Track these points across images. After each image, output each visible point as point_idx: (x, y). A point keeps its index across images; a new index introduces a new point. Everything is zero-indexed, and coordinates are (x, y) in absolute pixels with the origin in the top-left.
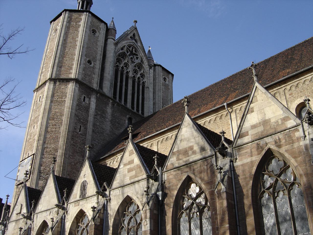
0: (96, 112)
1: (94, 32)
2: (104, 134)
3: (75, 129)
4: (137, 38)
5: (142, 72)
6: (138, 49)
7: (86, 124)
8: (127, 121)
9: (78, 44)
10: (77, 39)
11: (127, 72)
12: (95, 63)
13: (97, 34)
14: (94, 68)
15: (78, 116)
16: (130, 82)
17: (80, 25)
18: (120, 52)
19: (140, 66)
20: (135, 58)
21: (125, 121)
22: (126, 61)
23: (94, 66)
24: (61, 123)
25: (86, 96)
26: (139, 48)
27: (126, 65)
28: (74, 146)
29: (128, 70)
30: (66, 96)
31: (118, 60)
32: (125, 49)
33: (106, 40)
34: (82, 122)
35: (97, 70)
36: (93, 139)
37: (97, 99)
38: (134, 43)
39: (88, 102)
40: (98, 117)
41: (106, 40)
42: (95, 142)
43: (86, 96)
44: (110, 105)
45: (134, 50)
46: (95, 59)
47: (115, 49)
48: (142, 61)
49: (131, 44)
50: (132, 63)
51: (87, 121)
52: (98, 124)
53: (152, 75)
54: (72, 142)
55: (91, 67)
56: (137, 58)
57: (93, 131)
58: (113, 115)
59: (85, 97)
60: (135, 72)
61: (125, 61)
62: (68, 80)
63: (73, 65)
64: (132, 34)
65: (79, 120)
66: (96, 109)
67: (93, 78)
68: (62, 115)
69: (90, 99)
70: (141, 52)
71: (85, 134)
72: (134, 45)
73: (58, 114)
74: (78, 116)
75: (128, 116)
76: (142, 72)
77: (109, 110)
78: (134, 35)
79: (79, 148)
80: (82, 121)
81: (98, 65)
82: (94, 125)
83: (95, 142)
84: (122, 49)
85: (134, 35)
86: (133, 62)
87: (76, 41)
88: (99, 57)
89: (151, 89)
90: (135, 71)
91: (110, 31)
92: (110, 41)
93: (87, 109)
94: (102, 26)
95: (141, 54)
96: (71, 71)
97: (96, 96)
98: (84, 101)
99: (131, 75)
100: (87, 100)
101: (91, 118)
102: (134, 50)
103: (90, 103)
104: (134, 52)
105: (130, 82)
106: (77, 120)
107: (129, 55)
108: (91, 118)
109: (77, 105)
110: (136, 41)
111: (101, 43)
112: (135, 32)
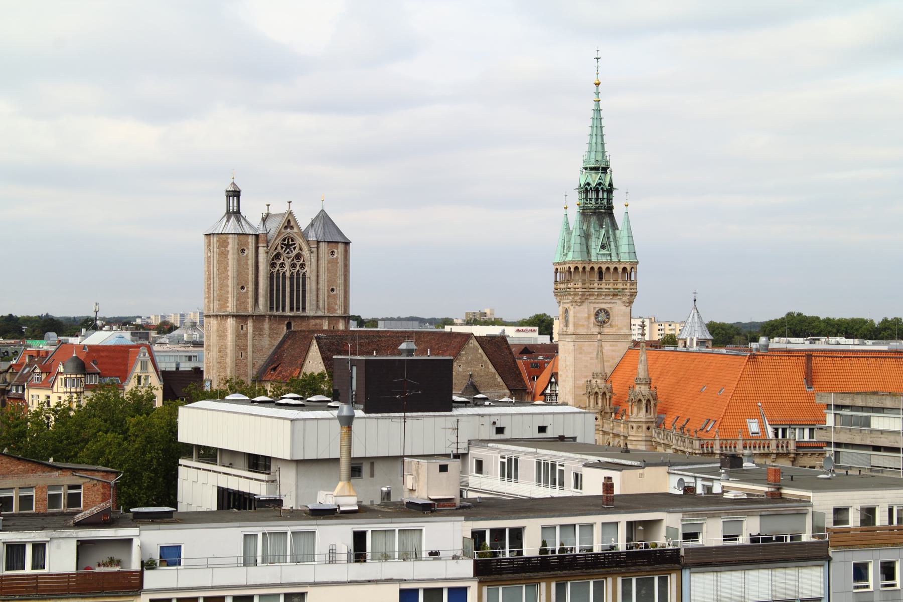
0: (254, 334)
1: (243, 251)
2: (264, 350)
3: (238, 357)
4: (292, 223)
5: (301, 262)
7: (247, 349)
8: (285, 328)
9: (230, 273)
10: (228, 268)
11: (284, 273)
12: (248, 286)
13: (246, 252)
14: (247, 292)
15: (238, 346)
16: (288, 282)
17: (228, 251)
18: (274, 254)
19: (298, 256)
20: (292, 249)
21: (283, 328)
22: (281, 261)
23: (247, 290)
24: (226, 355)
25: (243, 324)
26: (295, 235)
27: (282, 265)
28: (238, 370)
29: (284, 270)
30: (227, 331)
31: (273, 265)
32: (279, 247)
33: (257, 248)
34: (243, 349)
35: (251, 294)
36: (253, 358)
37: (254, 321)
39: (245, 329)
40: (256, 338)
41: (257, 248)
42: (256, 360)
43: (243, 324)
44: (267, 320)
45: (290, 240)
46: (247, 282)
47: (267, 257)
48: (301, 249)
49: (287, 236)
51: (247, 346)
52: (257, 344)
53: (314, 260)
54: (237, 369)
55: (245, 292)
56: (294, 248)
57: (253, 352)
58: (270, 329)
59: (242, 326)
60: (293, 266)
61: (279, 263)
62: (227, 316)
63: (228, 298)
64: (286, 224)
65: (240, 348)
66: (253, 331)
67: (248, 303)
68: (226, 348)
69: (247, 325)
70: (299, 239)
71: (247, 358)
73: (224, 347)
74: (238, 346)
75: (286, 322)
76: (301, 262)
77: (266, 325)
79: (243, 370)
80: (242, 348)
81: (251, 287)
82: (254, 346)
83: (256, 360)
84: (276, 248)
85: (289, 221)
86: (288, 258)
87: (228, 271)
88: (251, 277)
89: (314, 278)
91: (260, 237)
92: (262, 250)
93: (246, 335)
94: (250, 237)
95: (299, 241)
96: (228, 304)
97: (253, 319)
98: (242, 329)
99: (288, 274)
100: (244, 328)
101: (250, 343)
102: (290, 240)
103: (247, 329)
104: (290, 243)
105: (288, 282)
106: (238, 349)
107: (285, 251)
108: (250, 343)
109: (237, 336)
110: (292, 228)
111: (251, 262)
112: (290, 218)
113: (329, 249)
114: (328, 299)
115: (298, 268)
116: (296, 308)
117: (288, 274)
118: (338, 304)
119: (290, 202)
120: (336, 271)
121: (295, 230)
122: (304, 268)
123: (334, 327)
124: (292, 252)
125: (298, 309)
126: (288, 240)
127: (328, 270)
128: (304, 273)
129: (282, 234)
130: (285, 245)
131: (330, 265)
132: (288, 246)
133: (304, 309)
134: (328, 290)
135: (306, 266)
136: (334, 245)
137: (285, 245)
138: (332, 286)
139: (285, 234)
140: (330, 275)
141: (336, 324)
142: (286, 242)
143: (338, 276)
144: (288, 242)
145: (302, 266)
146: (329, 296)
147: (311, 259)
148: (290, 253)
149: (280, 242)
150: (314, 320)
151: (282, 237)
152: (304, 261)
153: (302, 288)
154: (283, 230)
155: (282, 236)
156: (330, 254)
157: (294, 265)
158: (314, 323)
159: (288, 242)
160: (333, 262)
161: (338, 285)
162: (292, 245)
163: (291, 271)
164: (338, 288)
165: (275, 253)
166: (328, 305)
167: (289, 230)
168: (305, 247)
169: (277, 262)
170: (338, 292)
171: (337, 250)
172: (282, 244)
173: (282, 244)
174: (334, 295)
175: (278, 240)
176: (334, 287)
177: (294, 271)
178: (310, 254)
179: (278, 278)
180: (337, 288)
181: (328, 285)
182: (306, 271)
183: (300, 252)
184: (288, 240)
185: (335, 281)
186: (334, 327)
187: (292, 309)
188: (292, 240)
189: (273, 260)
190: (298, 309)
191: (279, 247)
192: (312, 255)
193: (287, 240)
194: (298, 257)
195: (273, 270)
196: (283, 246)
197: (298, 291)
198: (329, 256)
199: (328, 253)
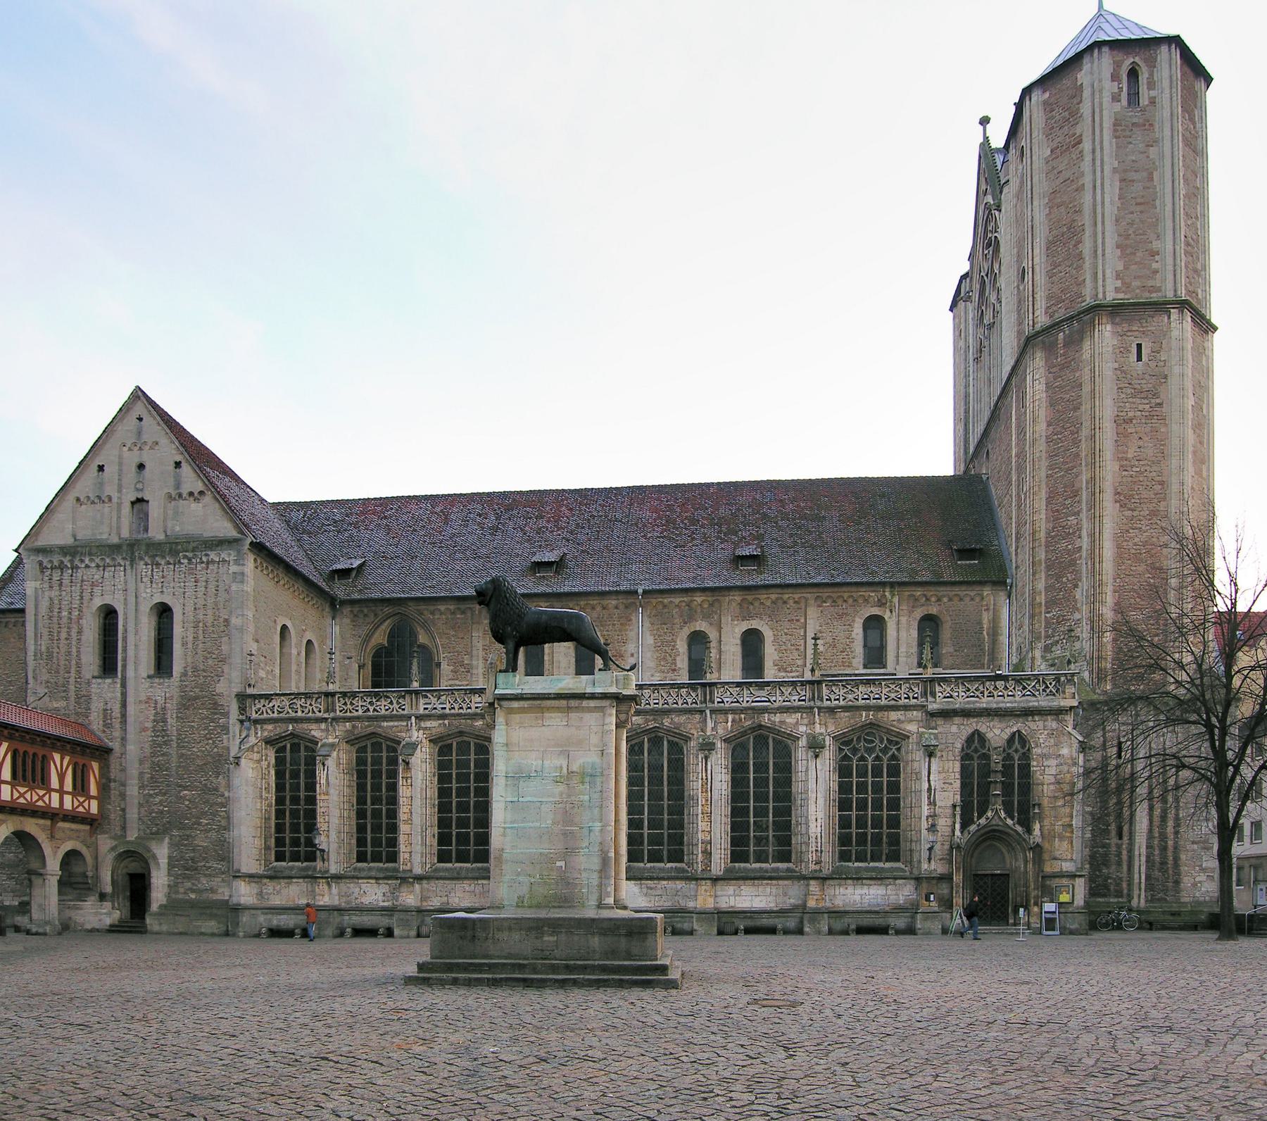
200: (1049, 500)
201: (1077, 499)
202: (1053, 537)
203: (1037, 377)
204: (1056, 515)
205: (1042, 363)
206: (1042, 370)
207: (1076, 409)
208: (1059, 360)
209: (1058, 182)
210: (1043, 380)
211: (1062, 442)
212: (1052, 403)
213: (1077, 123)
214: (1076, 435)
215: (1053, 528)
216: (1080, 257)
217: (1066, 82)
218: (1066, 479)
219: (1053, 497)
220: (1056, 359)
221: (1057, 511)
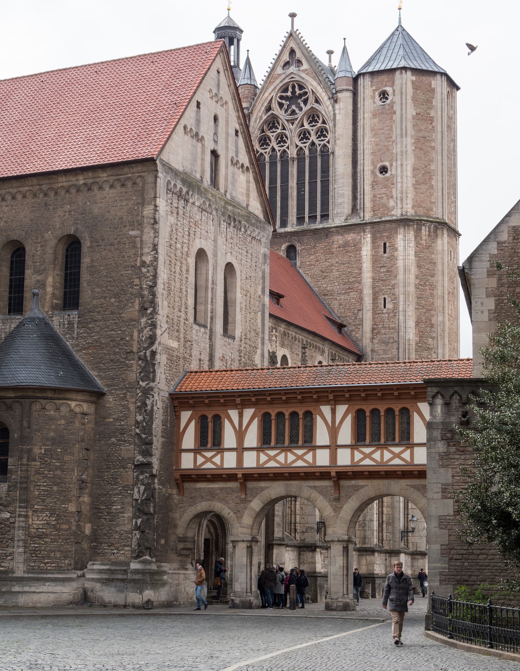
4: (299, 55)
6: (303, 78)
20: (302, 105)
26: (303, 75)
38: (292, 73)
49: (287, 80)
50: (293, 124)
56: (305, 102)
60: (304, 135)
72: (292, 78)
75: (284, 247)
78: (292, 52)
85: (292, 52)
90: (305, 134)
104: (298, 92)
112: (292, 44)
113: (374, 88)
114: (373, 188)
115: (313, 138)
116: (309, 217)
117: (292, 153)
118: (395, 196)
119: (293, 16)
120: (391, 129)
121: (305, 66)
122: (325, 136)
123: (385, 244)
124: (301, 109)
125: (312, 218)
126: (294, 87)
127: (372, 130)
128: (325, 145)
129: (277, 78)
130: (286, 98)
131: (376, 120)
132: (293, 99)
133: (325, 216)
134: (373, 172)
135: (329, 133)
136: (384, 78)
137: (286, 98)
138: (381, 161)
139: (283, 76)
140: (376, 140)
141: (389, 237)
142: (289, 94)
143: (394, 138)
144: (293, 92)
145: (322, 133)
146: (374, 184)
147: (335, 115)
148: (297, 111)
149: (274, 94)
150: (341, 235)
151: (278, 83)
152: (324, 122)
153: (322, 177)
154: (279, 70)
155: (278, 81)
156: (377, 98)
157: (305, 134)
158: (341, 242)
159: (293, 92)
160: (382, 113)
161: (395, 159)
162: (300, 96)
163: (297, 146)
164: (394, 164)
165: (264, 117)
166: (373, 201)
167: (292, 69)
168: (324, 94)
169: (270, 135)
170: (394, 172)
171: (392, 86)
172: (281, 98)
173: (281, 98)
174: (387, 179)
175: (269, 90)
176: (387, 164)
177: (302, 145)
178: (333, 107)
179: (273, 164)
180: (391, 165)
181: (373, 163)
182: (328, 142)
183: (316, 106)
184: (294, 87)
185: (388, 150)
186: (385, 244)
187: (300, 220)
188: (301, 87)
189: (263, 131)
190: (312, 218)
191: (275, 106)
192: (337, 106)
193: (290, 89)
194: (313, 117)
195: (263, 151)
196: (284, 102)
197: (313, 184)
198: (374, 102)
199: (373, 97)
200: (417, 323)
201: (433, 329)
202: (420, 347)
203: (411, 245)
204: (421, 335)
205: (413, 239)
206: (413, 242)
207: (433, 276)
208: (422, 242)
209: (421, 135)
210: (414, 249)
211: (424, 291)
212: (419, 266)
213: (431, 109)
214: (432, 292)
215: (420, 341)
216: (432, 187)
217: (425, 79)
218: (426, 315)
219: (419, 322)
220: (421, 240)
221: (422, 332)
